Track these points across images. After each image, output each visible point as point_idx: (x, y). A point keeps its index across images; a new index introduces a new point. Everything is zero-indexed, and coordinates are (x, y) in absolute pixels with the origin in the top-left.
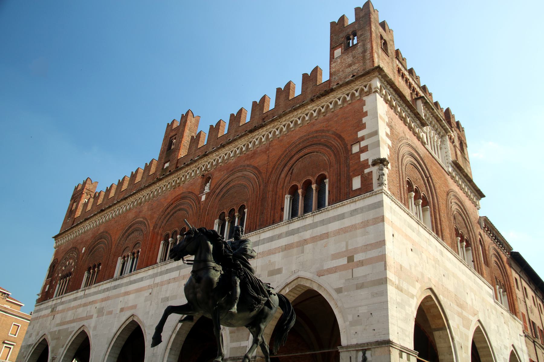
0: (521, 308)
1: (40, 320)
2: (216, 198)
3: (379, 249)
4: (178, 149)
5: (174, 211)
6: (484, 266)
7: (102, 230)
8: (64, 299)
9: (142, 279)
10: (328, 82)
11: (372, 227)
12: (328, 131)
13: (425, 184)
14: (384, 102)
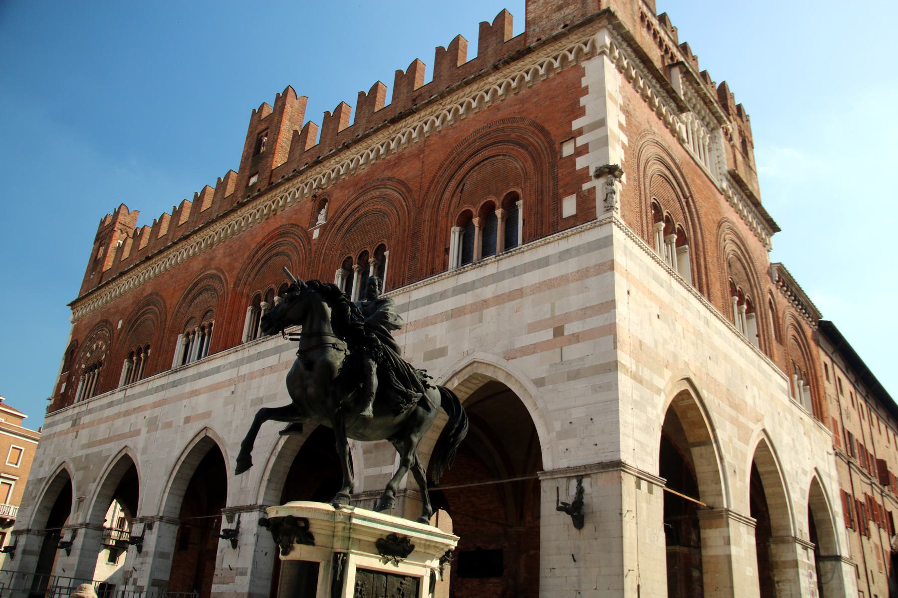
0: (831, 410)
1: (56, 439)
2: (336, 234)
3: (606, 315)
4: (271, 152)
5: (267, 256)
6: (775, 344)
7: (149, 290)
8: (92, 405)
9: (218, 370)
10: (523, 37)
11: (594, 279)
12: (523, 119)
13: (683, 209)
14: (616, 71)
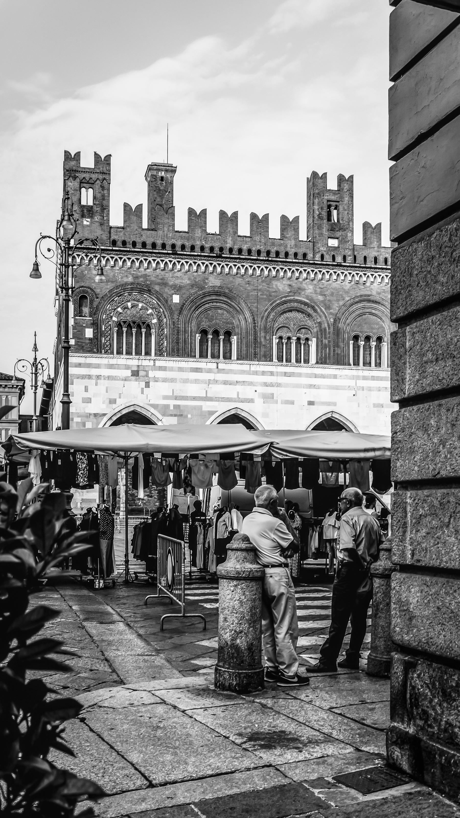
7: (214, 282)
8: (158, 363)
9: (335, 377)
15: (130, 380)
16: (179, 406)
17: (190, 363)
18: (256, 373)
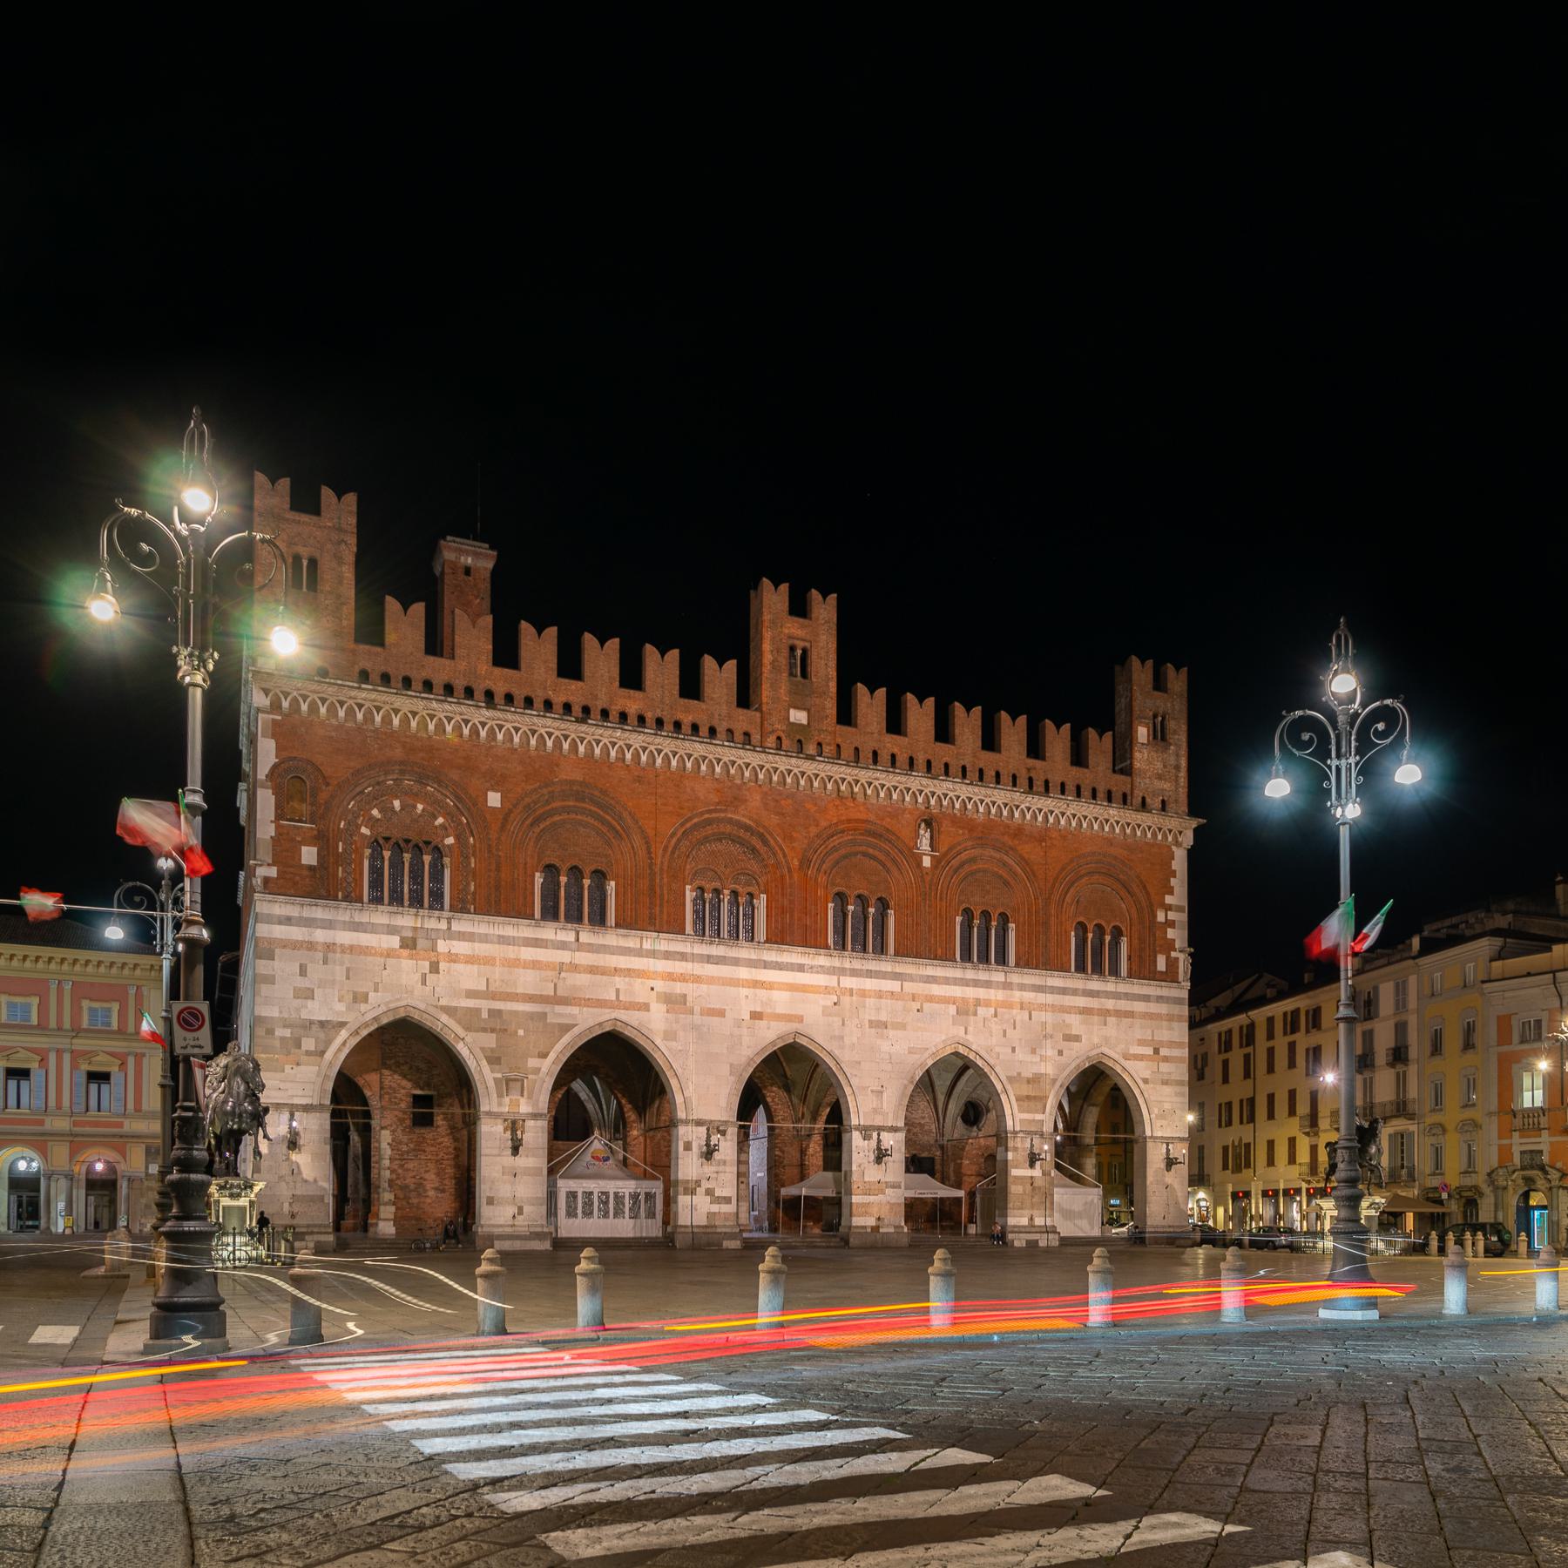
8: (456, 926)
9: (801, 968)
15: (399, 957)
16: (500, 1012)
17: (524, 930)
18: (653, 954)
